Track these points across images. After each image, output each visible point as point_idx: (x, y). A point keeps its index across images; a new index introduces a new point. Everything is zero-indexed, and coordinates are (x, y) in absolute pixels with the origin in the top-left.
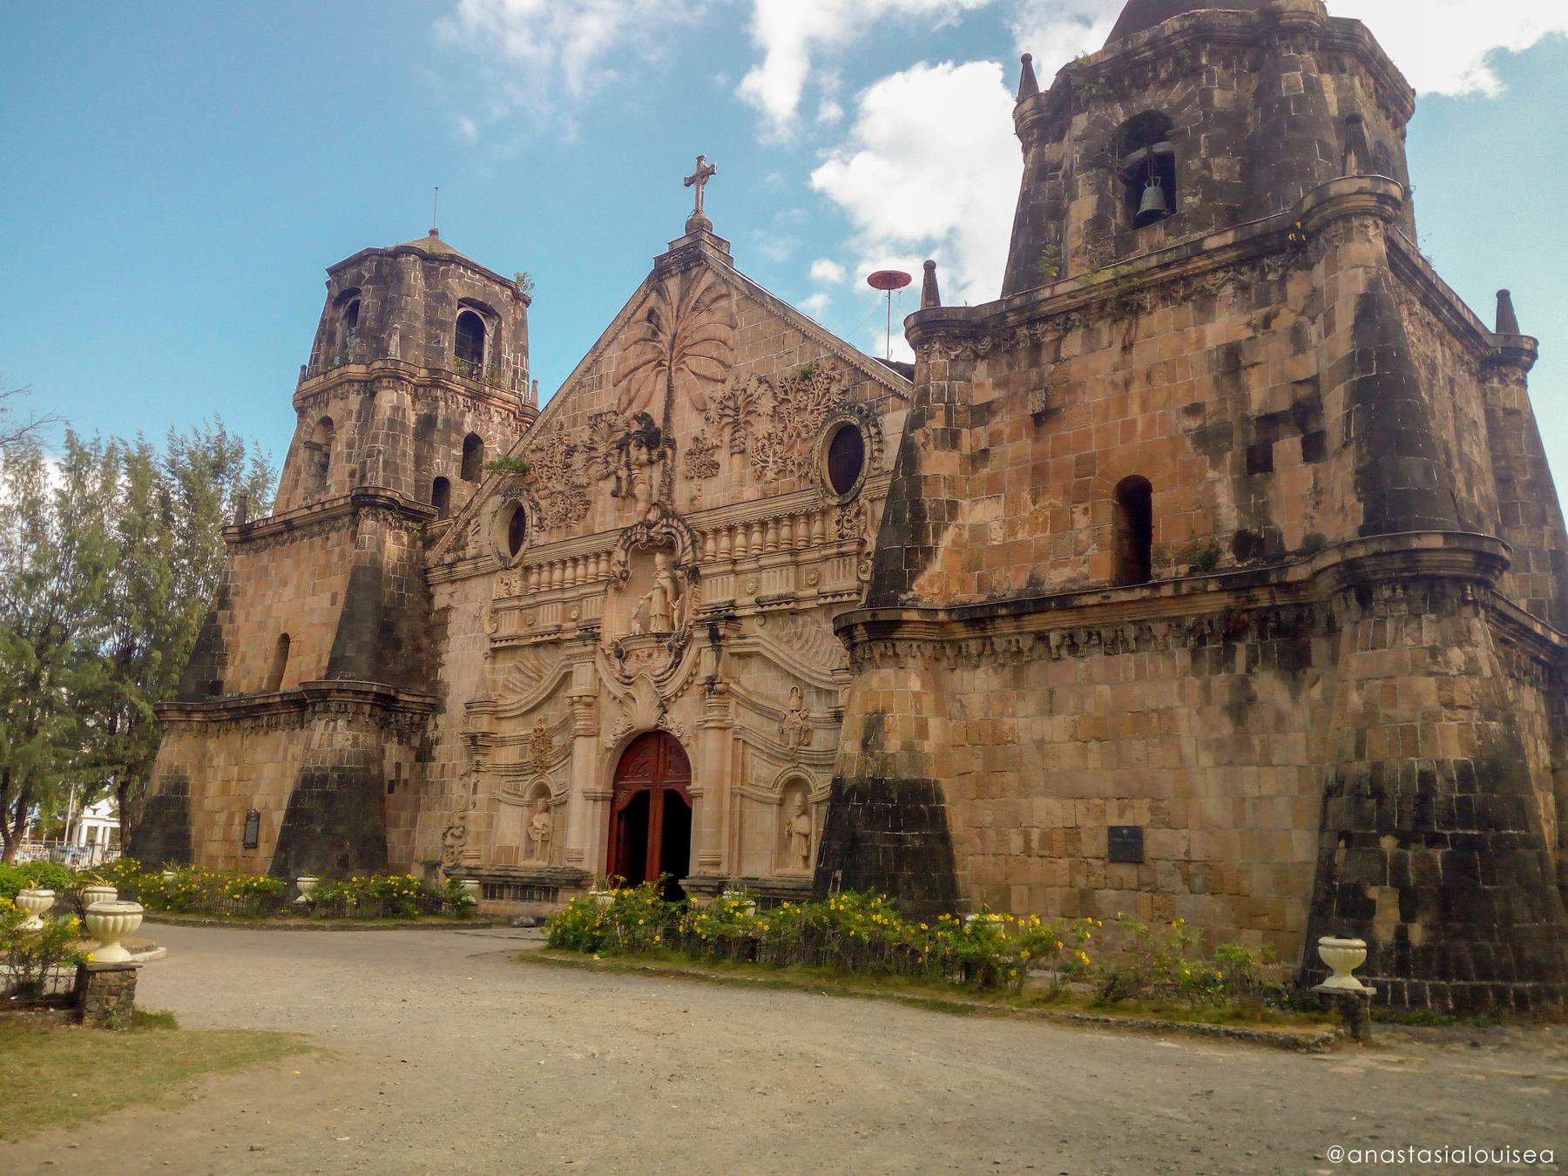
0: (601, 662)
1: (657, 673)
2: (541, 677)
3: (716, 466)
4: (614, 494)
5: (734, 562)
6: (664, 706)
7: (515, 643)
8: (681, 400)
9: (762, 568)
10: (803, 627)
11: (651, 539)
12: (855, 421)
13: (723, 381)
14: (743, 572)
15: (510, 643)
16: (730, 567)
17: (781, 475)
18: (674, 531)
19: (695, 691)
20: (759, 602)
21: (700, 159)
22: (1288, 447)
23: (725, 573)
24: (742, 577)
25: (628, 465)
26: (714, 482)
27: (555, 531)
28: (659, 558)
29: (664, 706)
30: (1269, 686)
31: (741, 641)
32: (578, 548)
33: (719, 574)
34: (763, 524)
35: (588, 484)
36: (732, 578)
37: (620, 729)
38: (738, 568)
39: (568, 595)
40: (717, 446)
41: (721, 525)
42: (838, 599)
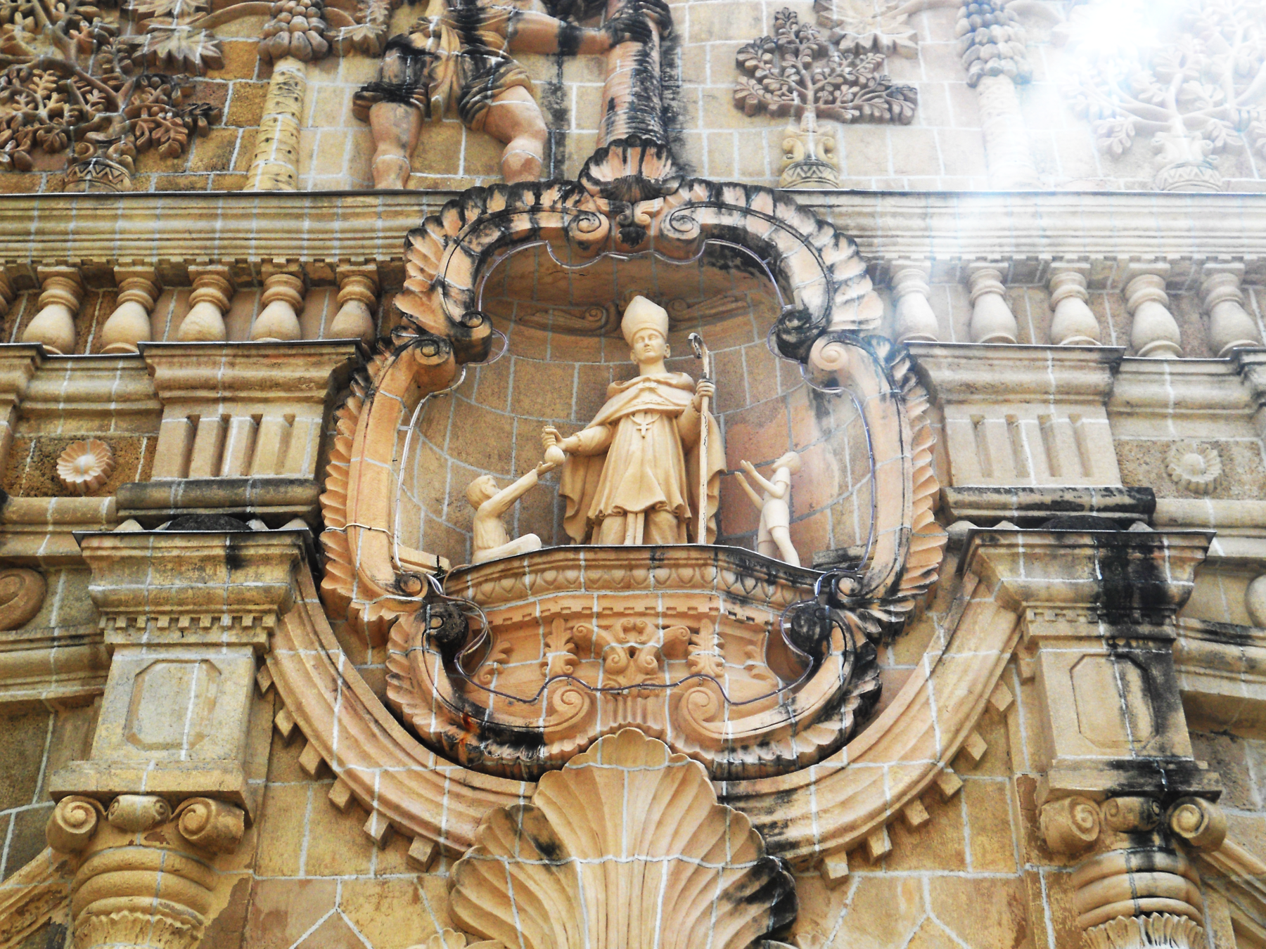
1: (731, 729)
3: (908, 94)
5: (1114, 362)
11: (634, 236)
14: (1153, 411)
16: (1099, 378)
17: (1228, 162)
23: (1069, 395)
24: (1137, 430)
26: (892, 133)
31: (1232, 651)
33: (1042, 394)
35: (210, 64)
36: (1095, 421)
38: (1130, 389)
40: (894, 49)
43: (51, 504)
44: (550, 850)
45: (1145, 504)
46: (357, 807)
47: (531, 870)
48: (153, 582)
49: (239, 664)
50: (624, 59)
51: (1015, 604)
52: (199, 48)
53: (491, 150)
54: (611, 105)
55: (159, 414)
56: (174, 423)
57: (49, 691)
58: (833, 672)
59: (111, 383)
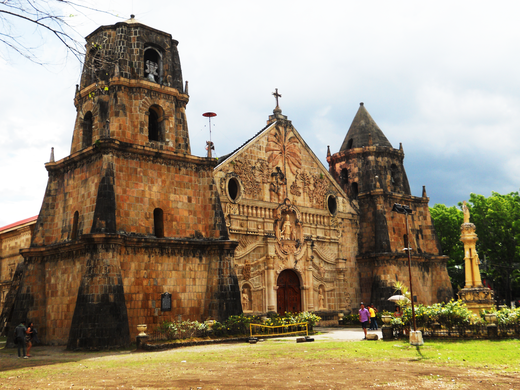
0: (277, 246)
2: (246, 246)
3: (300, 193)
4: (271, 190)
6: (296, 262)
7: (240, 232)
8: (287, 167)
9: (317, 228)
10: (324, 246)
12: (335, 197)
13: (300, 168)
15: (238, 232)
16: (310, 226)
18: (295, 210)
19: (303, 260)
20: (318, 237)
21: (277, 90)
22: (420, 236)
25: (277, 182)
27: (248, 195)
28: (288, 216)
29: (296, 262)
30: (426, 273)
32: (260, 204)
34: (313, 215)
36: (309, 229)
37: (282, 269)
39: (259, 220)
41: (304, 212)
42: (335, 241)
43: (259, 230)
44: (287, 259)
45: (312, 236)
46: (279, 256)
47: (286, 260)
48: (271, 241)
49: (274, 246)
50: (285, 186)
51: (307, 245)
52: (259, 181)
53: (277, 196)
54: (284, 192)
55: (264, 222)
56: (265, 224)
57: (262, 246)
58: (299, 249)
59: (261, 220)
